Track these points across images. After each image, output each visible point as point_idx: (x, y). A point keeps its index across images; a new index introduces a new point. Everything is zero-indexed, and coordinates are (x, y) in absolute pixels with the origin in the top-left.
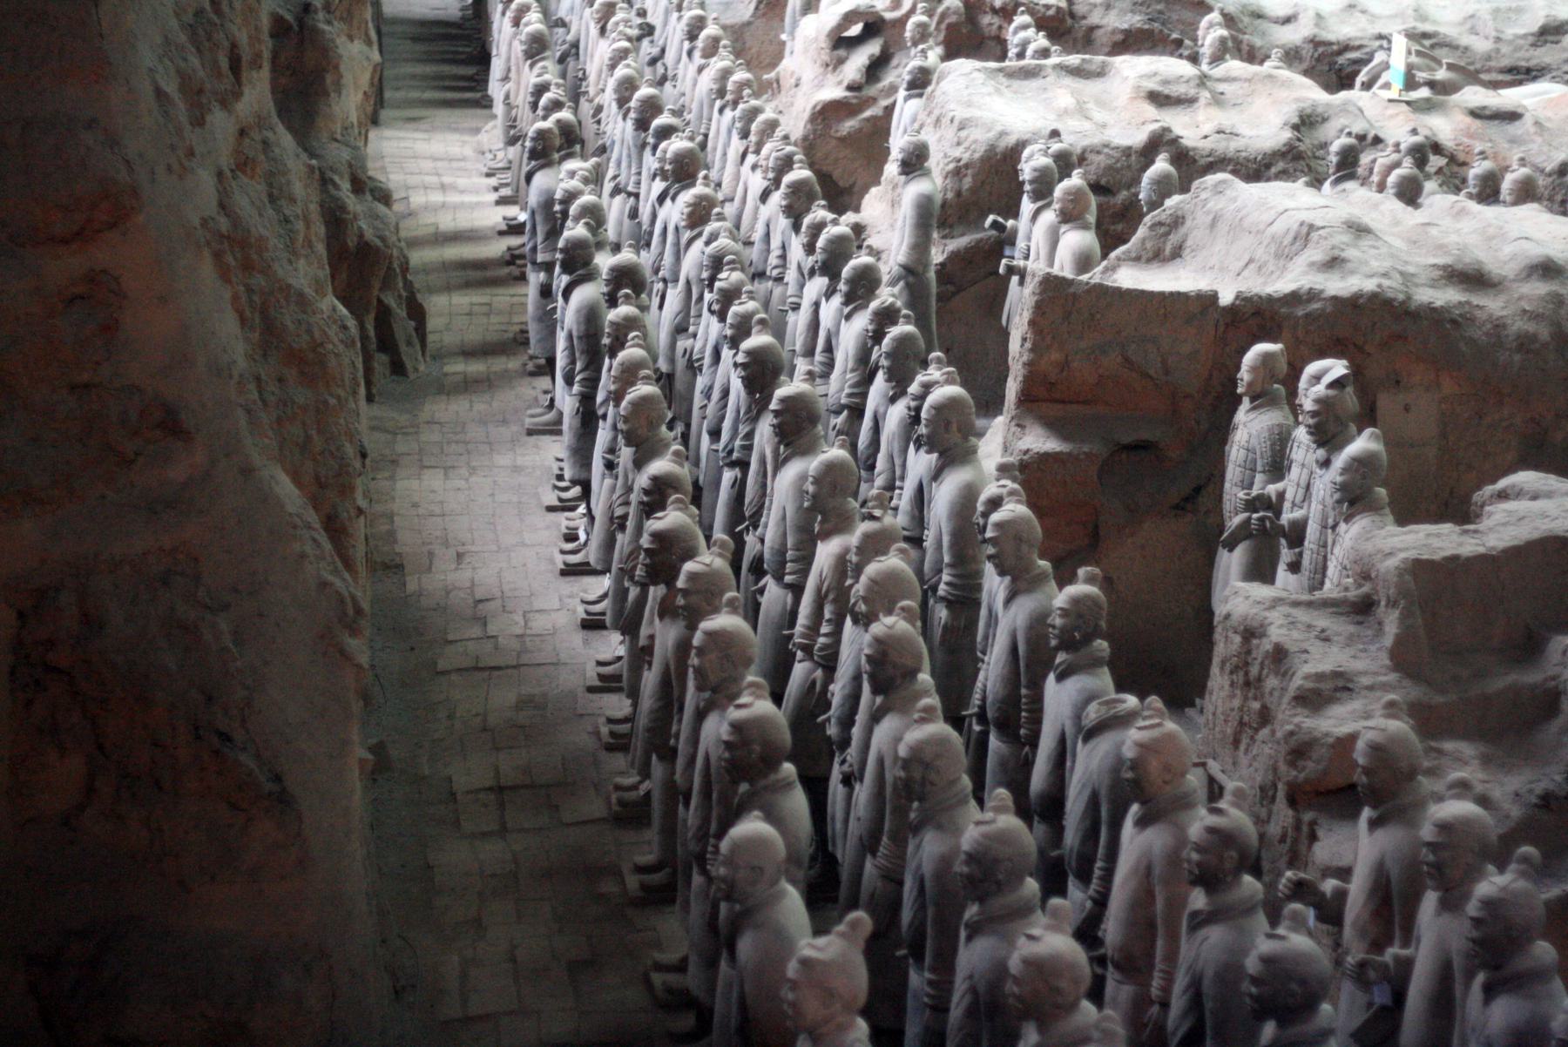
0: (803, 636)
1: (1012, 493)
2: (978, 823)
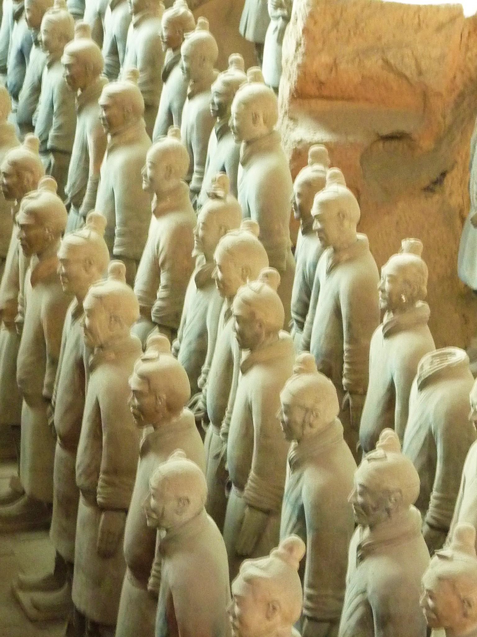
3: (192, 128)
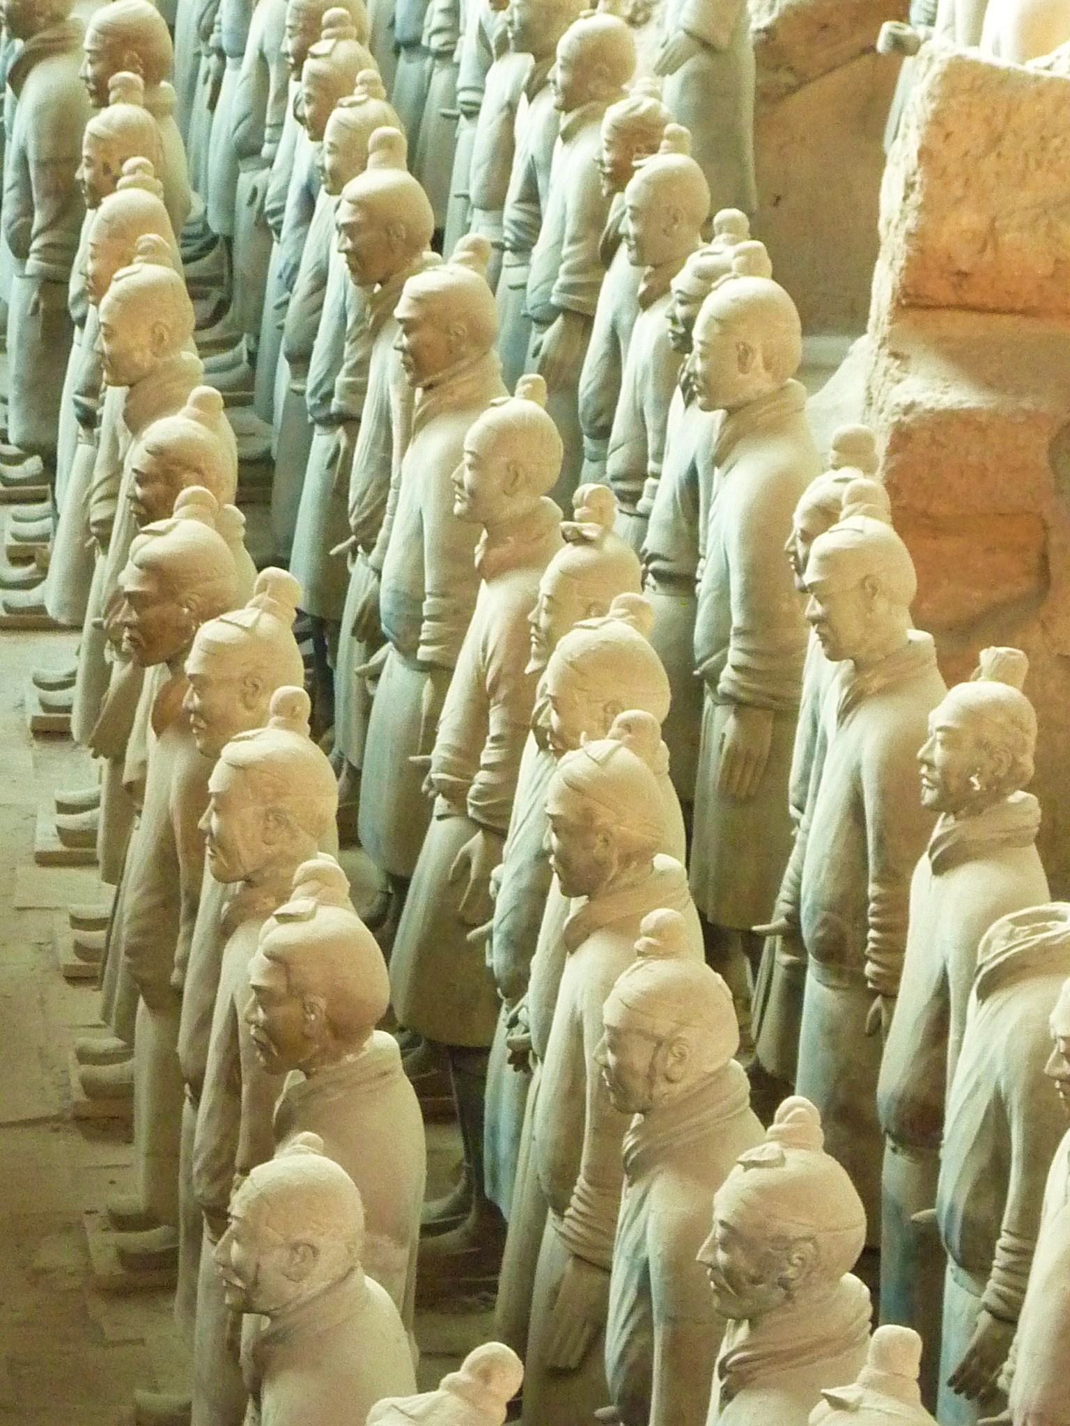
0: (447, 767)
1: (859, 496)
2: (749, 1165)
3: (645, 370)
